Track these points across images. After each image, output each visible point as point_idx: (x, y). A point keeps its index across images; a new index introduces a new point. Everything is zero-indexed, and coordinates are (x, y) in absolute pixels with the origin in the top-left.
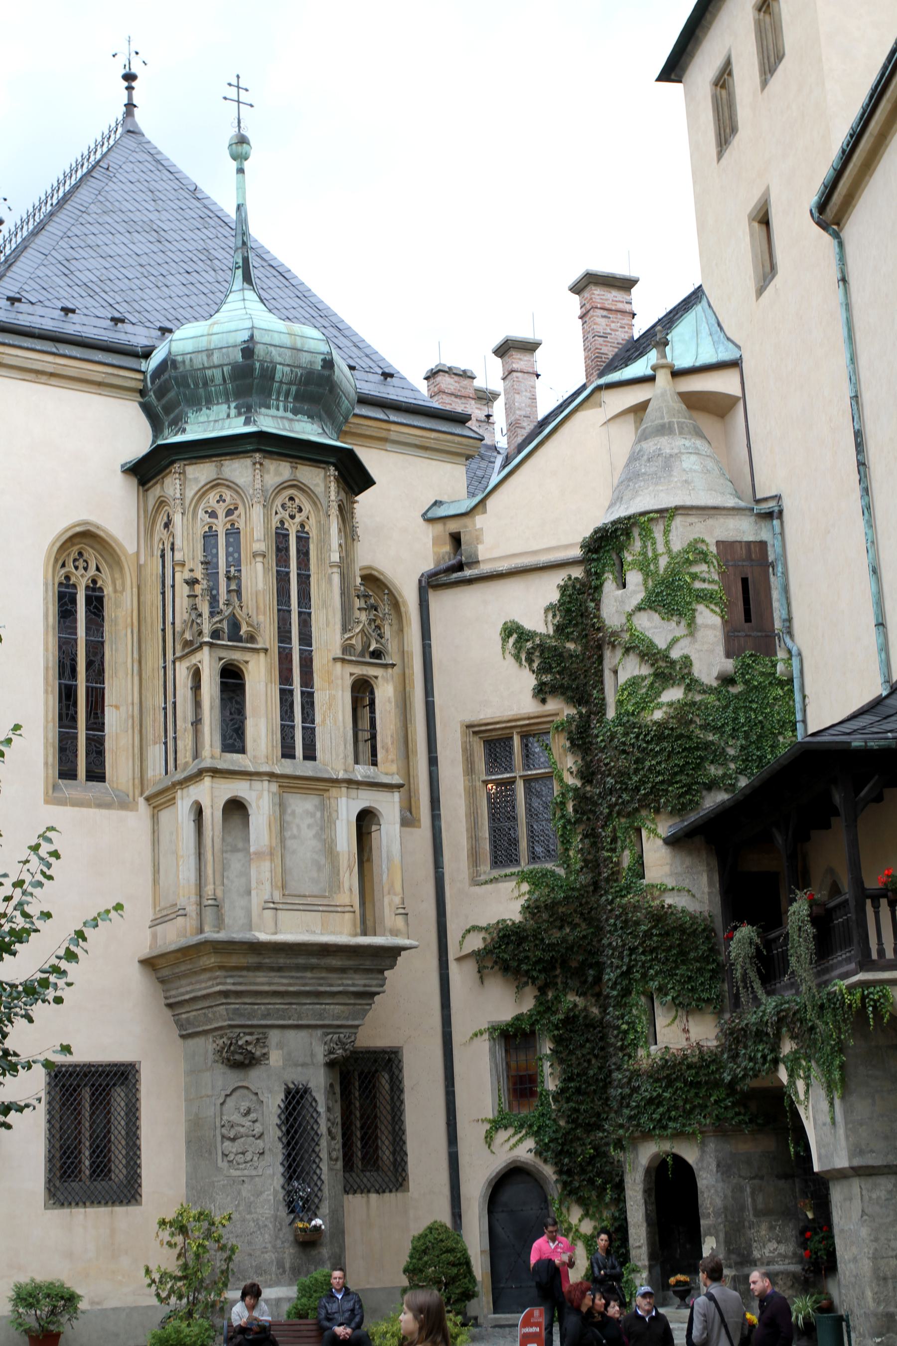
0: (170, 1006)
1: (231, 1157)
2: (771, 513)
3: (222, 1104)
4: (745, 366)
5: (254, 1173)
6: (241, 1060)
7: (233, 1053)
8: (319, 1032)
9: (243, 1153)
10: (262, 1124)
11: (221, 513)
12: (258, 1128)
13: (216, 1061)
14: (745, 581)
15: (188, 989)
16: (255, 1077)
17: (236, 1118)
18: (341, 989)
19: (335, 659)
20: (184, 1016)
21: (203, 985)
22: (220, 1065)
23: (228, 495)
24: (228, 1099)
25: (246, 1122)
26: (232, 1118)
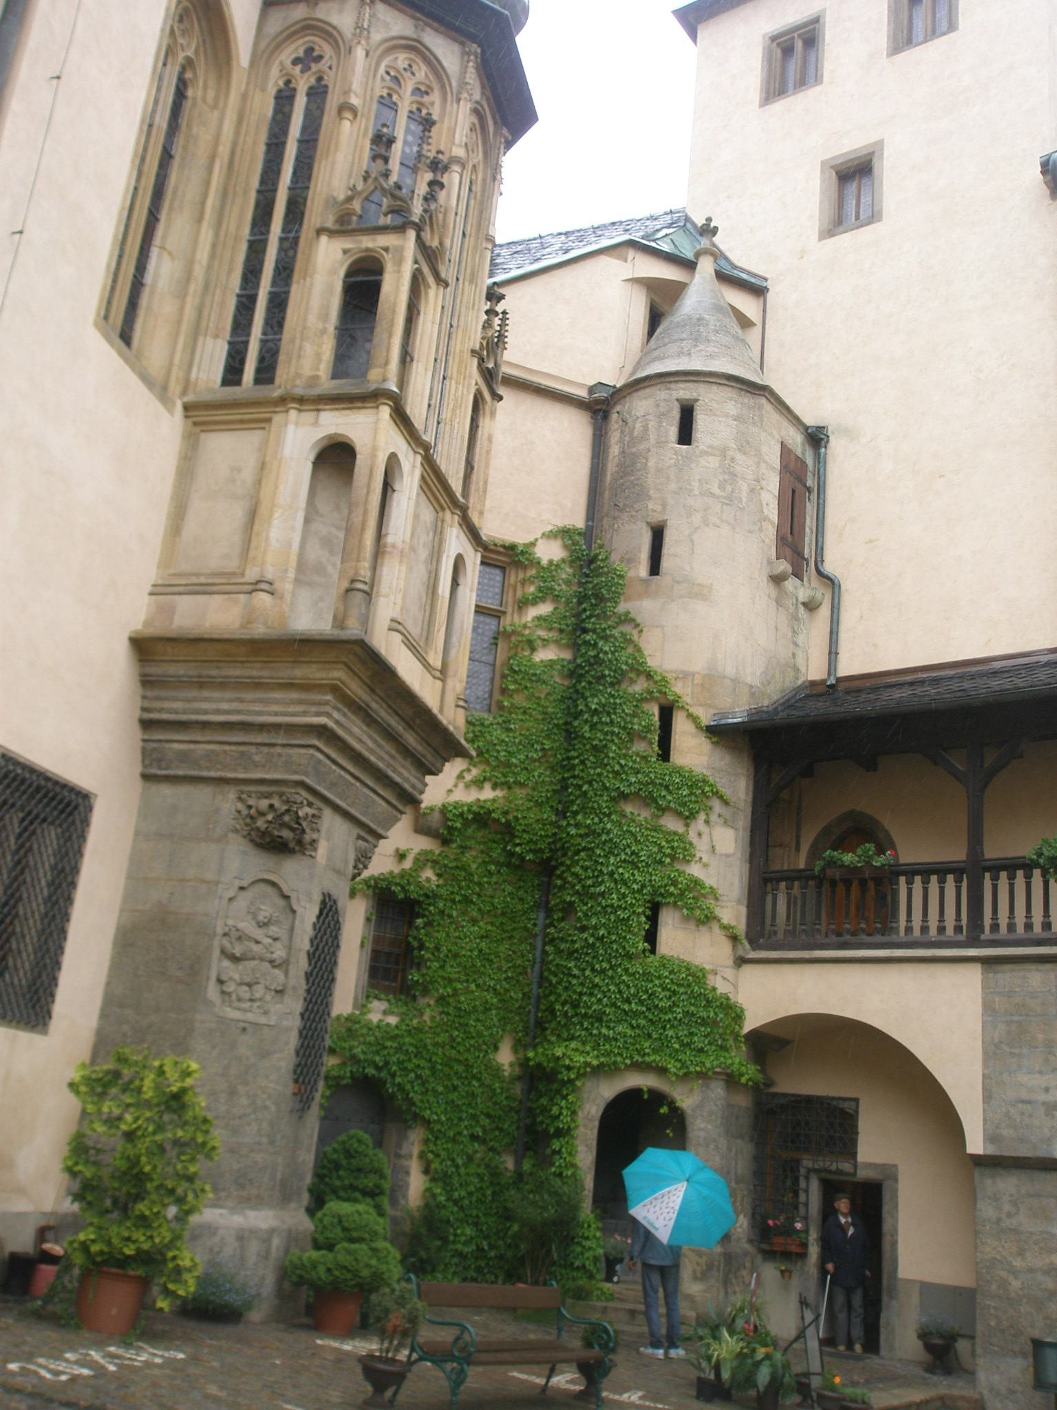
0: (146, 724)
1: (231, 987)
2: (816, 438)
3: (230, 899)
4: (770, 296)
5: (263, 1020)
6: (280, 839)
7: (284, 825)
8: (357, 831)
9: (249, 985)
10: (289, 948)
11: (409, 86)
12: (279, 953)
13: (236, 831)
14: (794, 491)
15: (225, 706)
16: (290, 871)
17: (247, 926)
18: (398, 779)
19: (473, 351)
20: (176, 746)
21: (275, 708)
22: (241, 840)
23: (422, 72)
24: (243, 893)
25: (258, 934)
26: (241, 925)
